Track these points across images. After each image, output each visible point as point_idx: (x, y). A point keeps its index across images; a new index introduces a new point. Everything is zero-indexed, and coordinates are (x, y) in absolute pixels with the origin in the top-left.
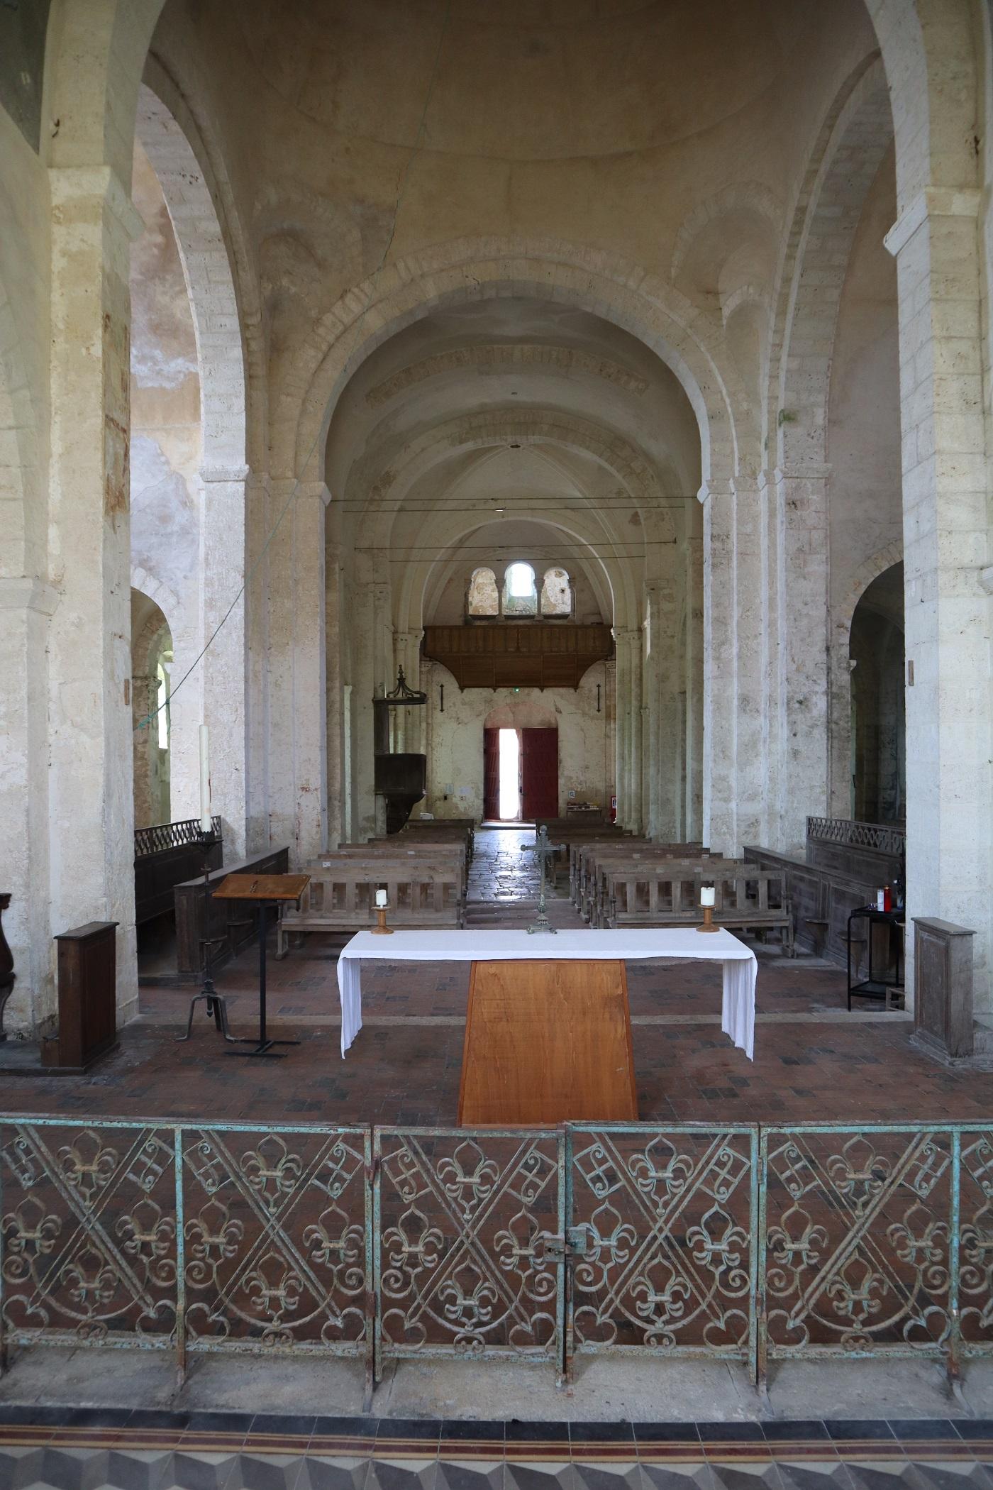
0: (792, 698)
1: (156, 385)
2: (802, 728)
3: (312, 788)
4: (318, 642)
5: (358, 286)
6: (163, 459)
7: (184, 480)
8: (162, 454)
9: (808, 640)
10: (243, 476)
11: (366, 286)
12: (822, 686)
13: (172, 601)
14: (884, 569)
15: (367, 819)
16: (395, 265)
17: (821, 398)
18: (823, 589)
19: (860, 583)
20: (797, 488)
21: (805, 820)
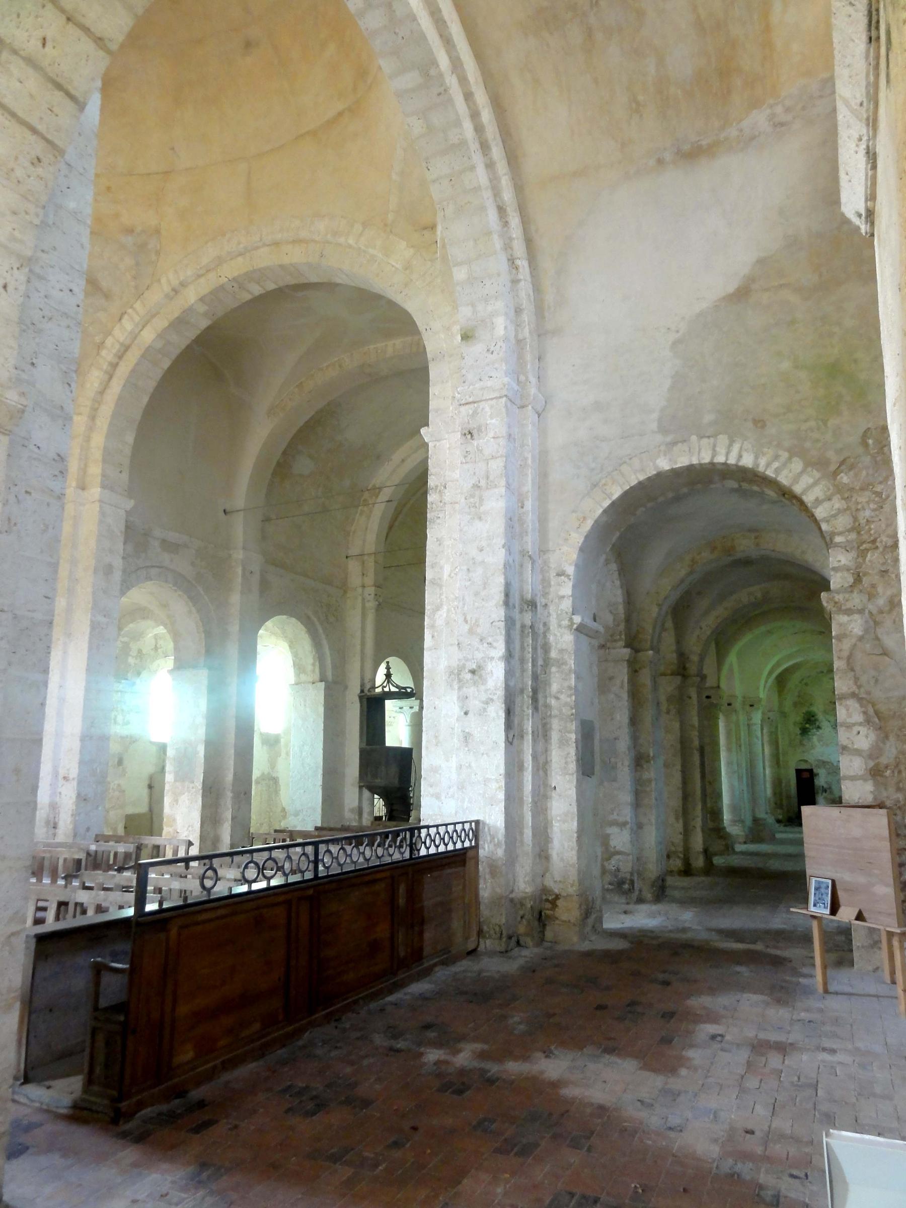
0: (464, 666)
2: (475, 704)
3: (71, 777)
5: (131, 307)
9: (483, 593)
11: (138, 305)
12: (500, 649)
14: (615, 496)
15: (352, 810)
16: (159, 281)
17: (500, 305)
18: (501, 530)
19: (584, 518)
20: (475, 413)
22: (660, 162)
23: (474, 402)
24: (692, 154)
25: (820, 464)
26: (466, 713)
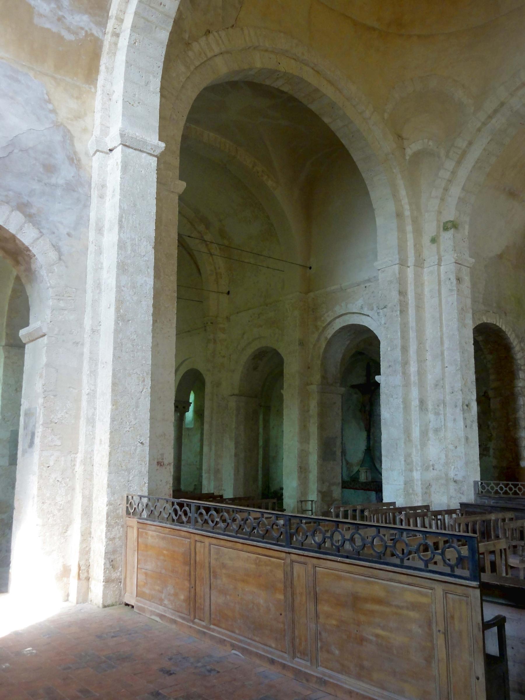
1: (54, 30)
3: (166, 462)
4: (174, 325)
6: (50, 107)
7: (72, 138)
8: (49, 101)
10: (157, 153)
11: (223, 34)
13: (53, 255)
21: (472, 484)
22: (505, 189)
23: (460, 264)
24: (512, 194)
25: (517, 336)
26: (466, 427)
